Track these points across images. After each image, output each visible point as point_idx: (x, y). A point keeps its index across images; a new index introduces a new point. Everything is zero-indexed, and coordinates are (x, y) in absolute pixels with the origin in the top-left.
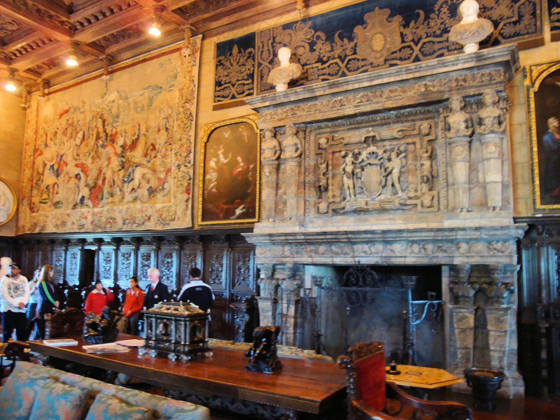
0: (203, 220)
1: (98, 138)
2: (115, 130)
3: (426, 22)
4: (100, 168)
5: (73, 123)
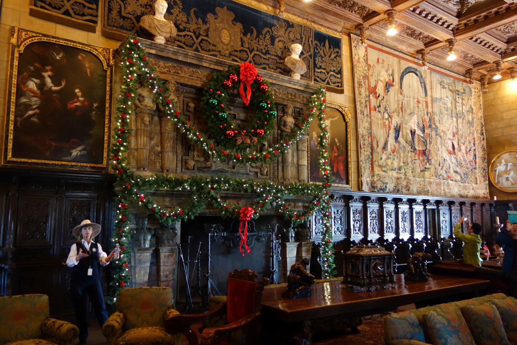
0: (13, 156)
3: (257, 39)
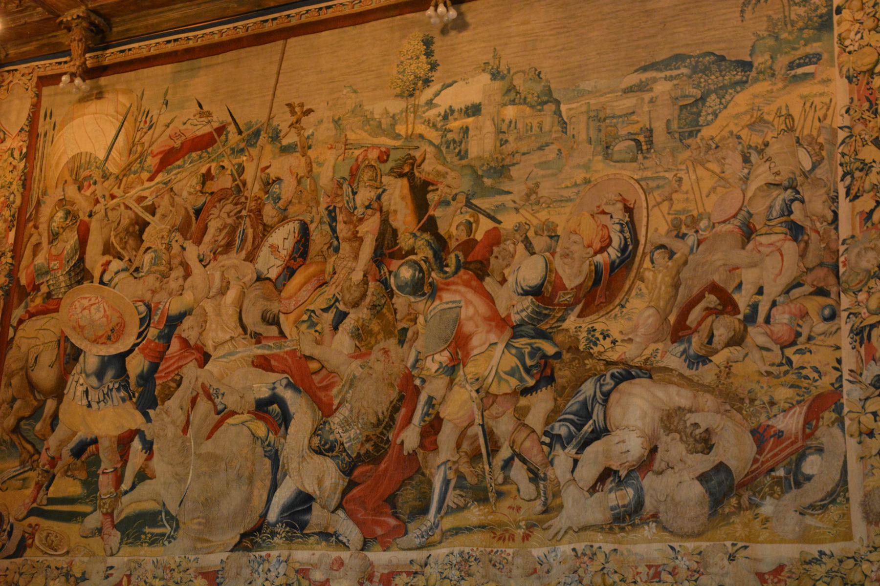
1: (387, 248)
2: (485, 225)
4: (408, 378)
5: (239, 190)
